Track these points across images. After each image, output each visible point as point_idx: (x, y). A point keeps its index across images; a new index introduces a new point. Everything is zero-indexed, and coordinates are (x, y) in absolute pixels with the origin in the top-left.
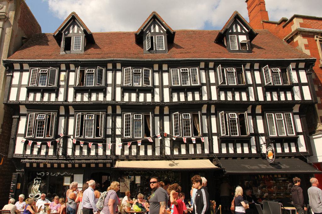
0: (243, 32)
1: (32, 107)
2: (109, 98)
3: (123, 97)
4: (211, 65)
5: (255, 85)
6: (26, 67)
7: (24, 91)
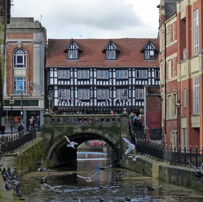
0: (153, 49)
1: (60, 87)
2: (91, 83)
3: (97, 83)
4: (133, 69)
5: (151, 78)
6: (56, 69)
7: (56, 80)
